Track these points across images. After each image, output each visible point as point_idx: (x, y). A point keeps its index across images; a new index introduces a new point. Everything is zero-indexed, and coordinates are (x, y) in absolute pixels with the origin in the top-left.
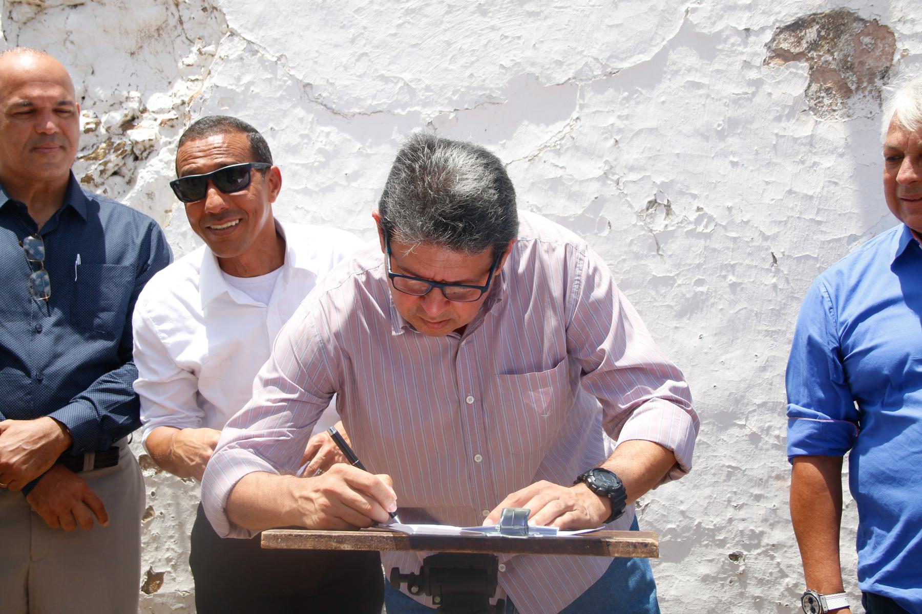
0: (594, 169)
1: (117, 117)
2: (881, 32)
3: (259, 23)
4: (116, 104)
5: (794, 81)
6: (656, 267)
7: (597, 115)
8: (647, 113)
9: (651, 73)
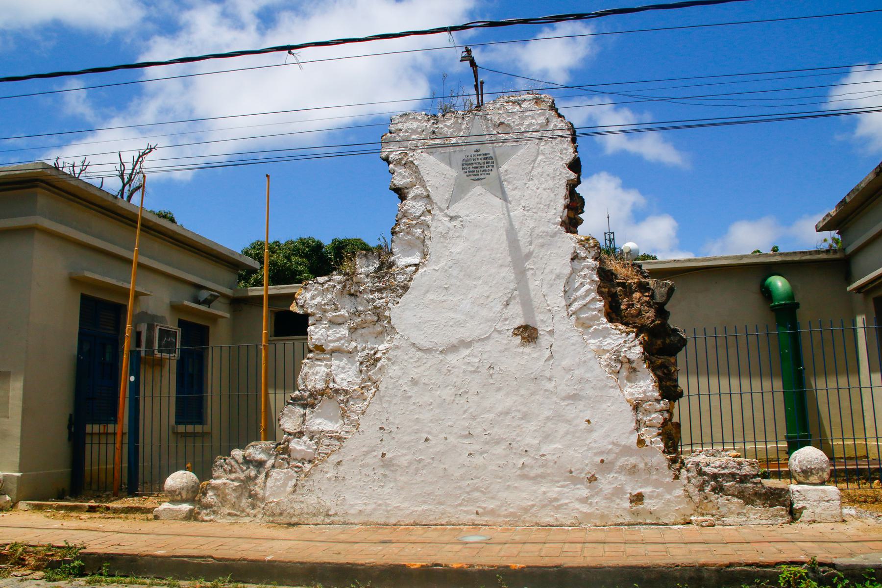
0: (477, 360)
1: (373, 352)
2: (535, 329)
3: (403, 331)
4: (372, 349)
5: (518, 340)
6: (491, 381)
7: (477, 348)
8: (488, 348)
9: (487, 338)
